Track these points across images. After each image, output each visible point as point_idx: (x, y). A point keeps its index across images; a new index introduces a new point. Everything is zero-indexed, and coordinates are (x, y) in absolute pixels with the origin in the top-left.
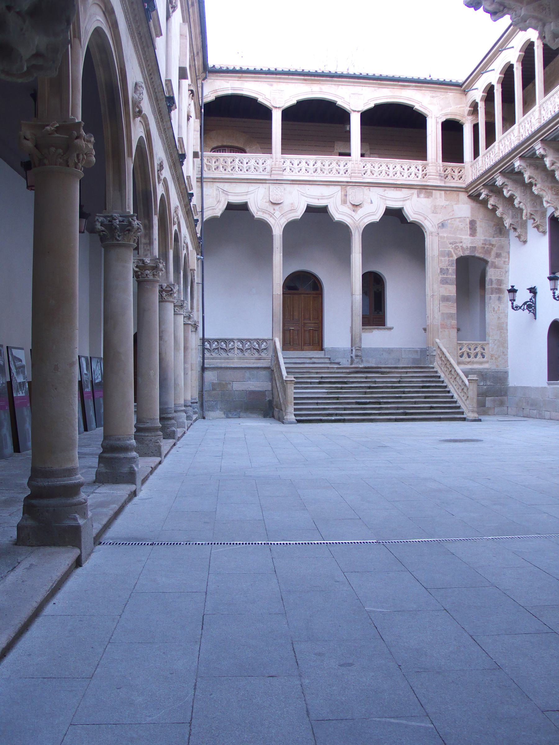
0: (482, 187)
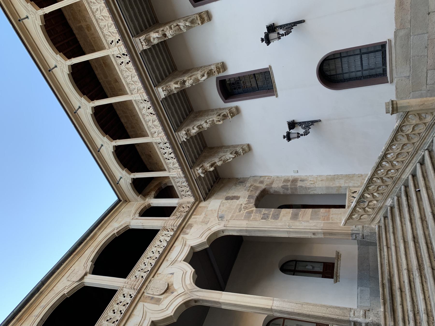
0: (192, 170)
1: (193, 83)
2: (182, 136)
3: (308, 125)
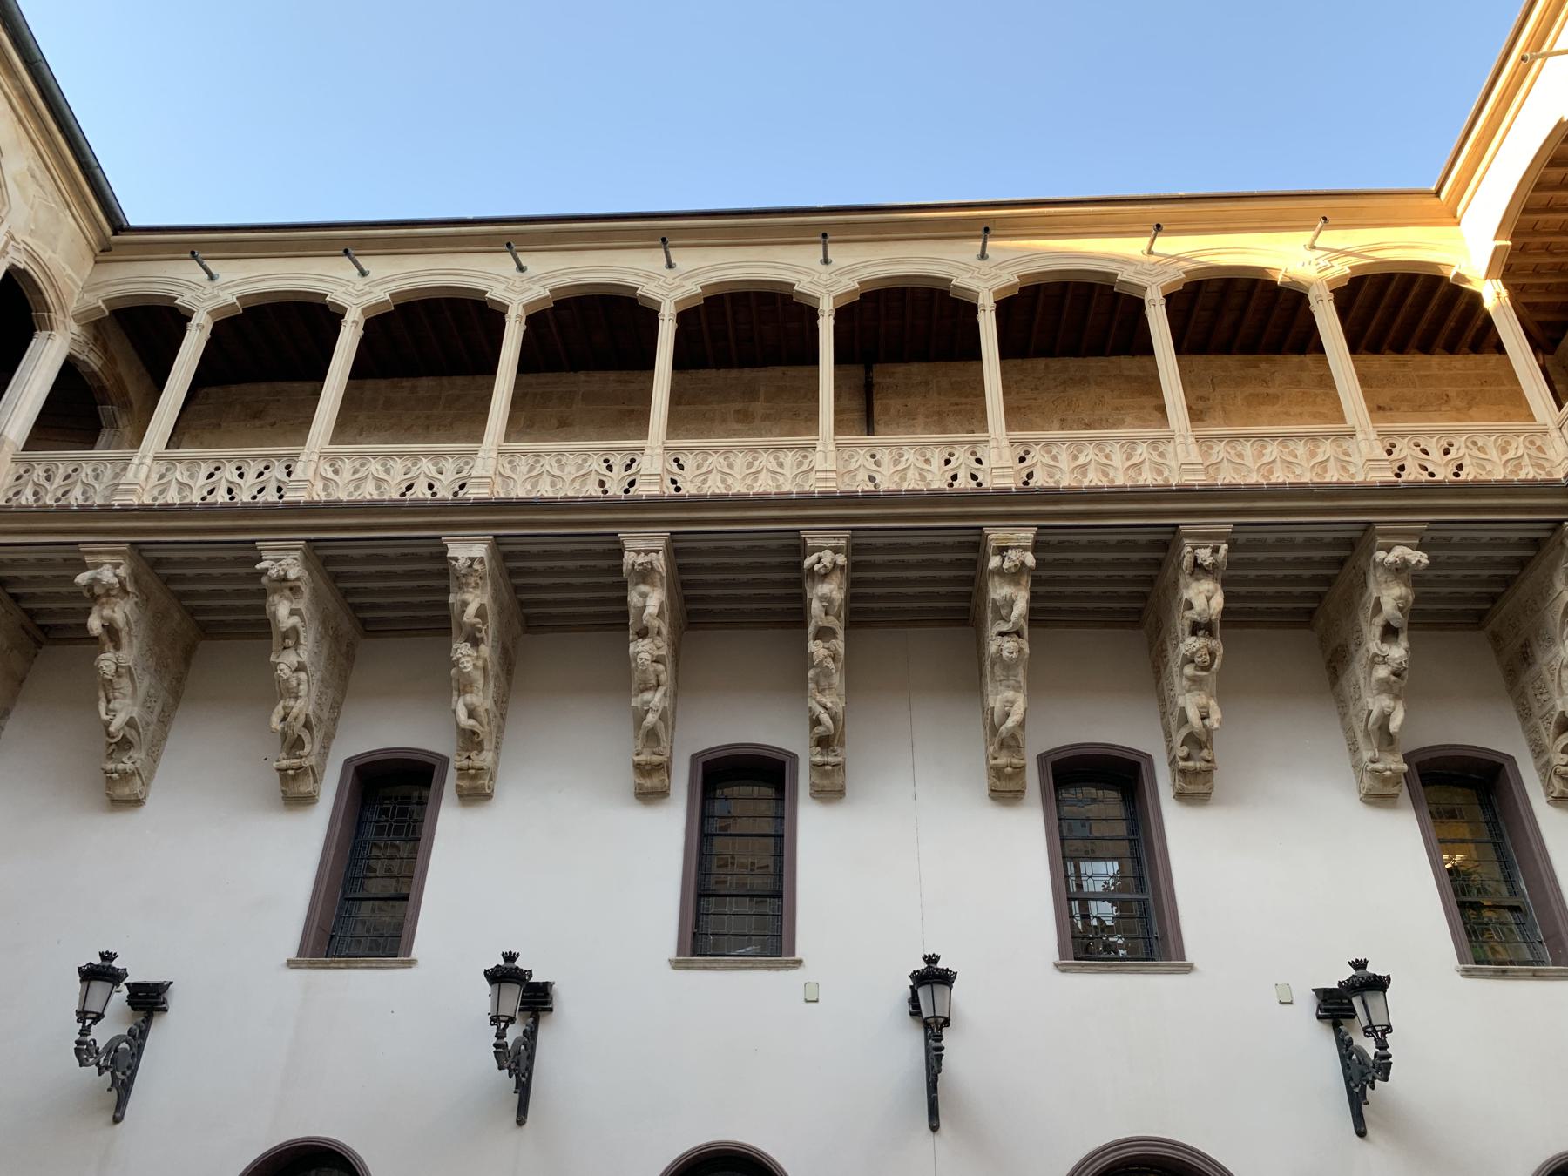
0: (124, 547)
1: (460, 671)
2: (283, 560)
3: (119, 1068)
